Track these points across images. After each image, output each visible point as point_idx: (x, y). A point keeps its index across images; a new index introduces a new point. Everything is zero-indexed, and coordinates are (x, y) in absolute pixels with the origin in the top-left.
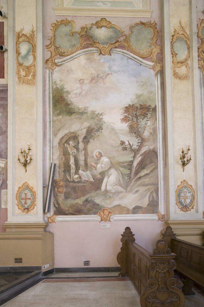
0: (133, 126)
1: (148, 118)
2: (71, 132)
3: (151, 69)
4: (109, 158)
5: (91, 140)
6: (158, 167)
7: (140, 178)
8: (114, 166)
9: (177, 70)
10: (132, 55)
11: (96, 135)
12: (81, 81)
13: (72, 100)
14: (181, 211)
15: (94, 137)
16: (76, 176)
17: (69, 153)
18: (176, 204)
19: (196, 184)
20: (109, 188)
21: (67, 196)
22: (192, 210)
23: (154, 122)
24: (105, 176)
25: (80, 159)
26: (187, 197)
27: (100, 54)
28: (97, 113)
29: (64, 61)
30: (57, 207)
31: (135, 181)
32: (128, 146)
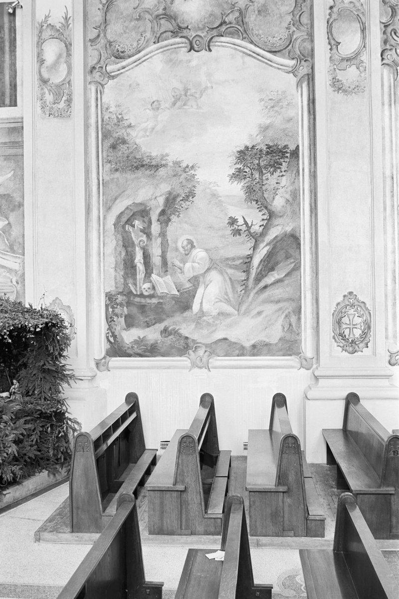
0: (252, 188)
1: (281, 172)
2: (137, 204)
3: (289, 72)
4: (206, 250)
5: (174, 218)
6: (300, 266)
7: (266, 287)
8: (215, 265)
9: (340, 75)
10: (252, 47)
11: (182, 207)
12: (155, 106)
13: (138, 141)
14: (344, 351)
15: (178, 212)
16: (147, 285)
17: (133, 243)
18: (334, 338)
19: (374, 299)
20: (206, 307)
21: (130, 323)
22: (365, 350)
23: (295, 179)
24: (199, 285)
25: (154, 253)
26: (355, 325)
27: (190, 51)
28: (184, 165)
29: (124, 68)
30: (113, 341)
31: (257, 293)
32: (244, 228)
